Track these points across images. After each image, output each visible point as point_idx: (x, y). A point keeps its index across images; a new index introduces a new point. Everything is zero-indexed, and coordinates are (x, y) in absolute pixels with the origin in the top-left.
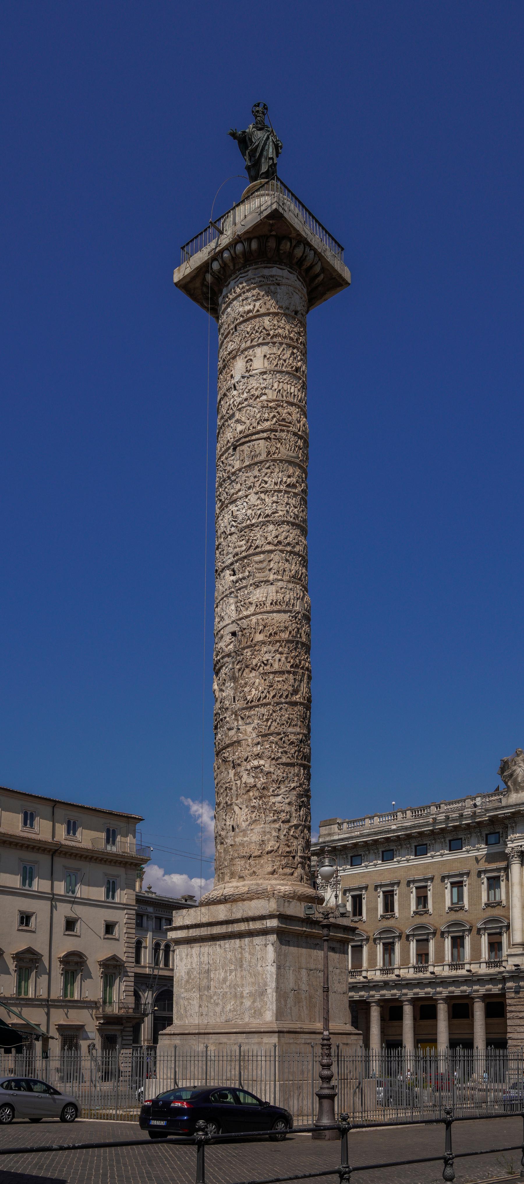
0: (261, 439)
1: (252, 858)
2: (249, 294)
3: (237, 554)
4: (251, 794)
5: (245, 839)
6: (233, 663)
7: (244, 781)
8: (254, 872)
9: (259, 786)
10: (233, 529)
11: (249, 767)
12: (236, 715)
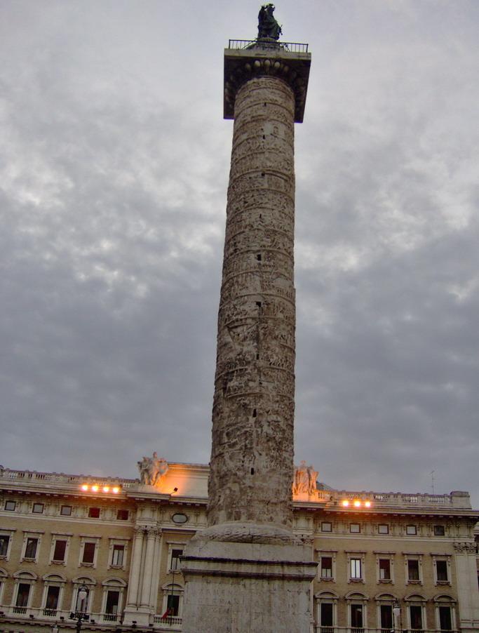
0: (283, 178)
1: (270, 504)
2: (278, 92)
3: (264, 246)
4: (270, 444)
5: (264, 484)
6: (258, 327)
7: (264, 431)
8: (271, 518)
9: (277, 439)
10: (260, 227)
11: (269, 420)
12: (259, 371)
